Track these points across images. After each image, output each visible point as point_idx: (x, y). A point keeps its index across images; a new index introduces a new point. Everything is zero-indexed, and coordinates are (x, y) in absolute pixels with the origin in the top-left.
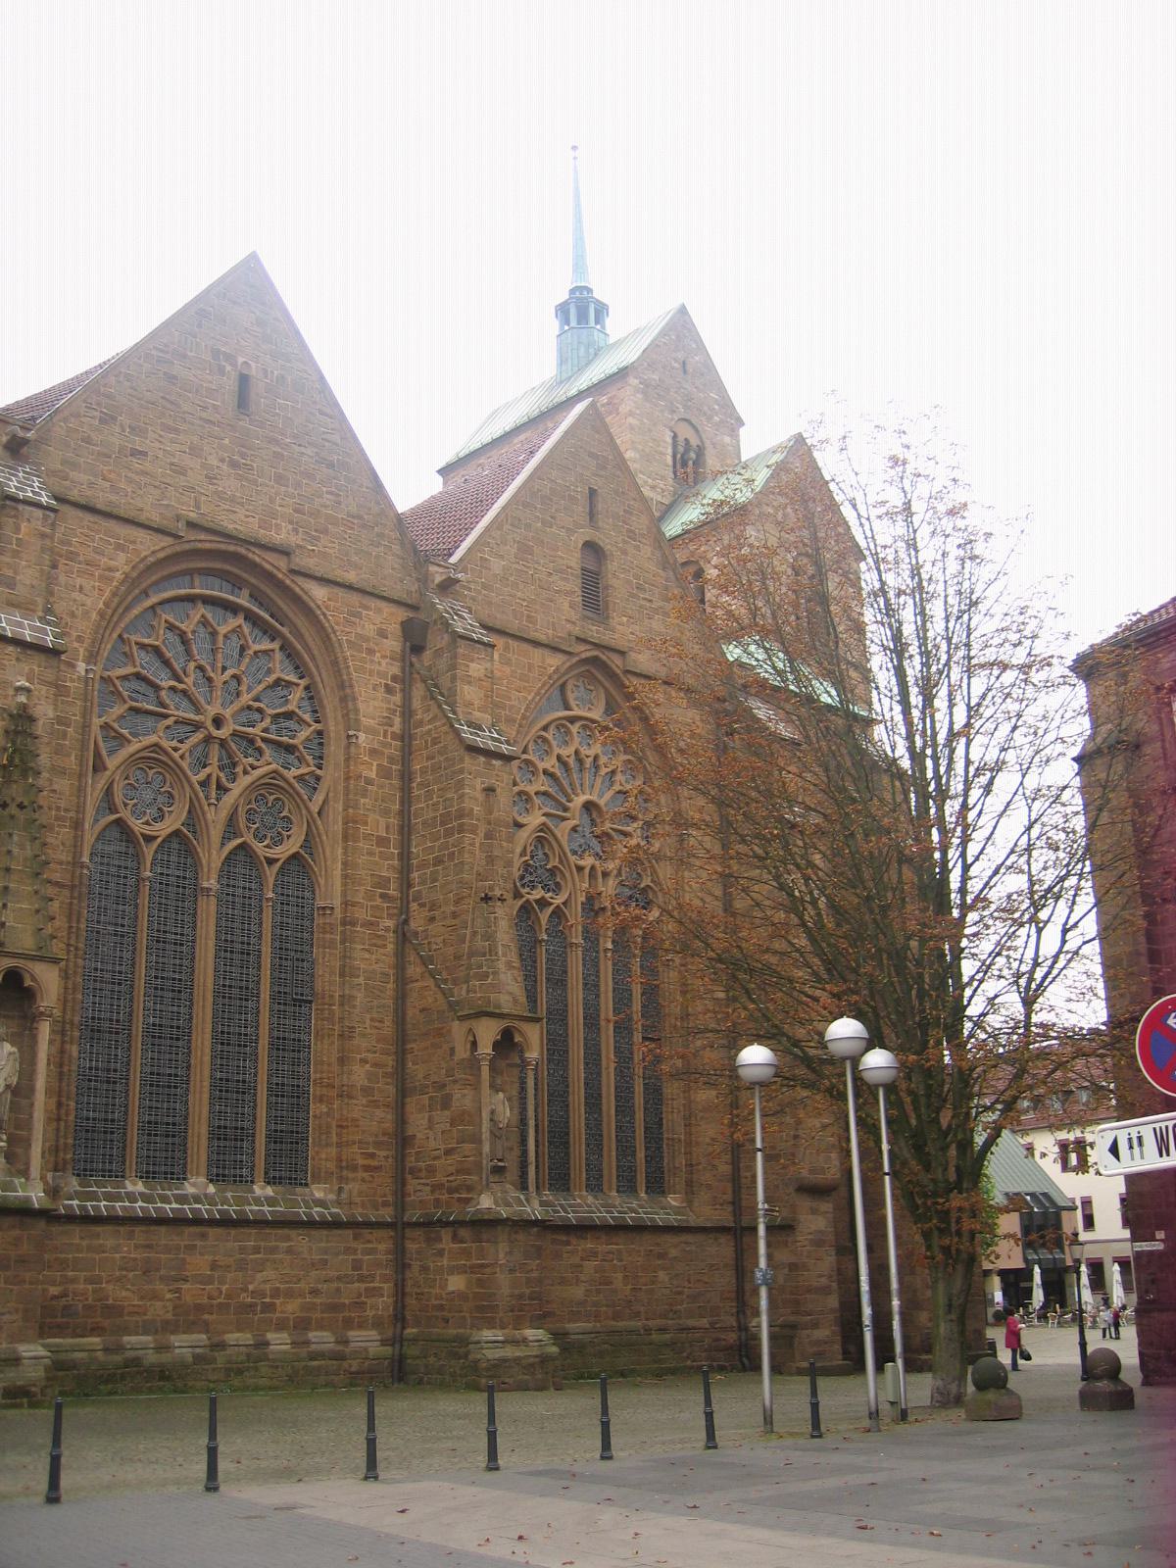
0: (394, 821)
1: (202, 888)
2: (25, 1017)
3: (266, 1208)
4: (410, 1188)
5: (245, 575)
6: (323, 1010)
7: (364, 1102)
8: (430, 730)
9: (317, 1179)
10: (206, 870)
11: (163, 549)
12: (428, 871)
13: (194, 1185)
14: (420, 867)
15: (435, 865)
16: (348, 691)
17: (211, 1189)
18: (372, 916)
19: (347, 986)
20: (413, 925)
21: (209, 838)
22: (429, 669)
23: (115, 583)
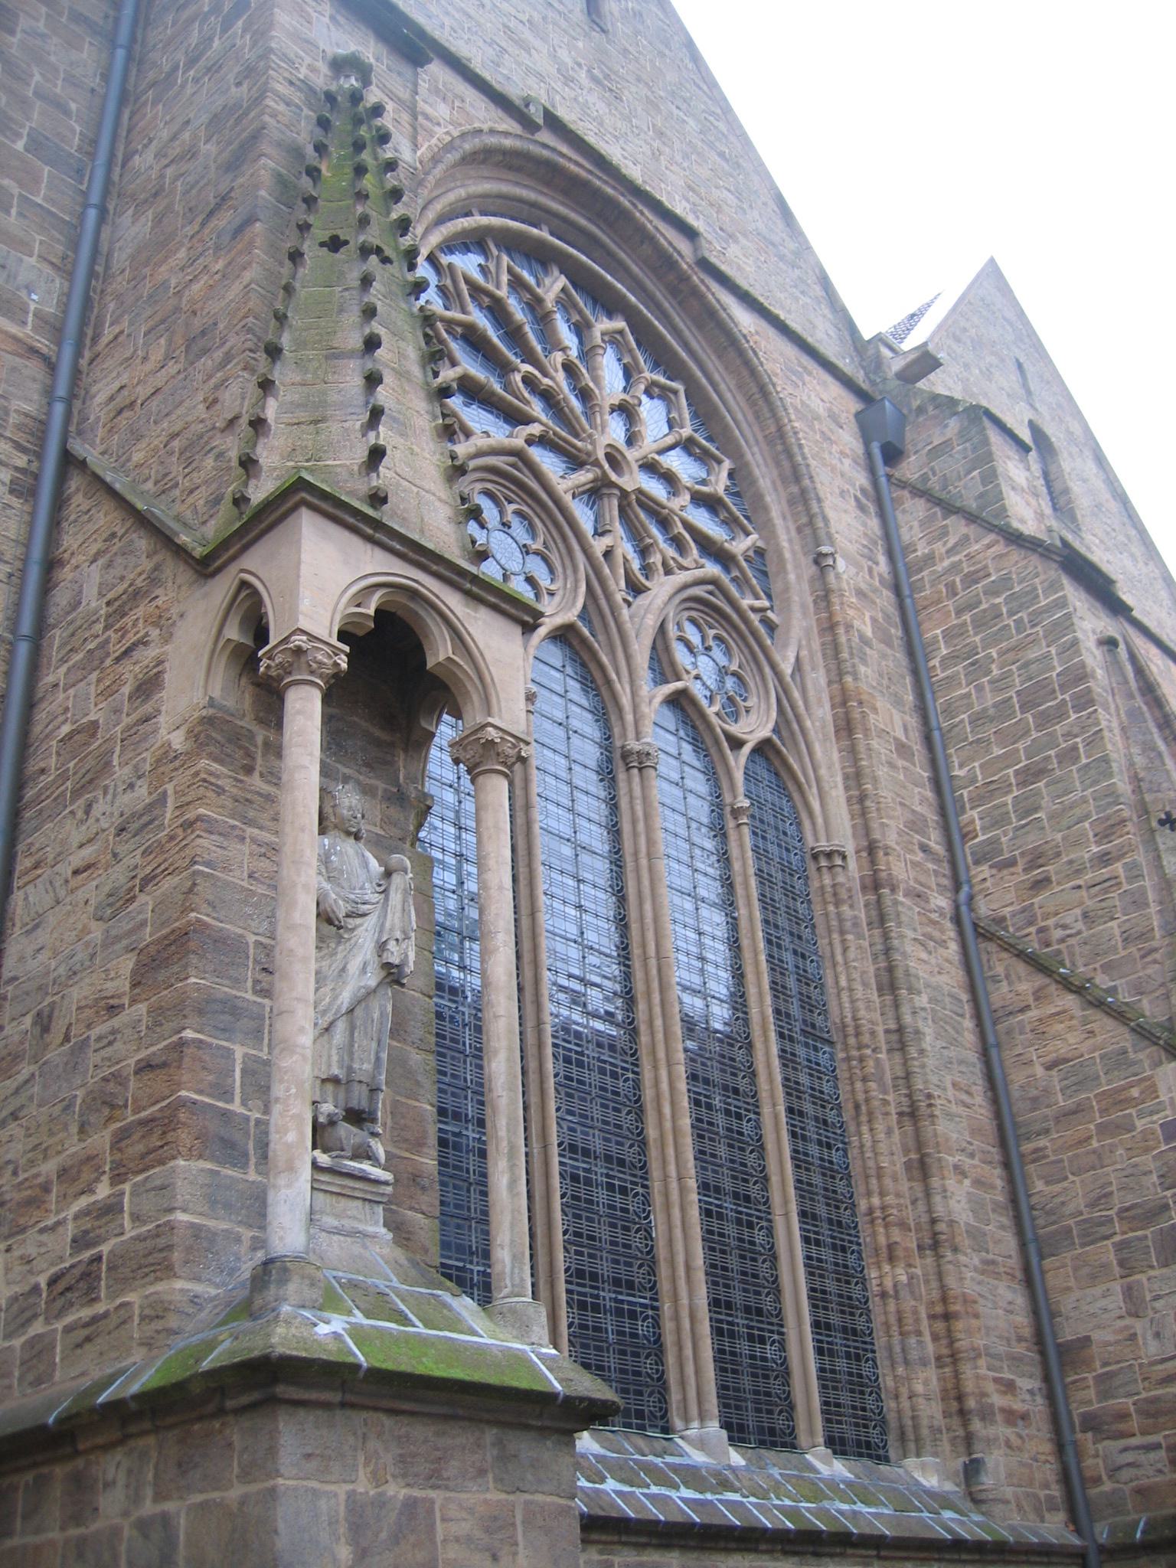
0: (913, 721)
1: (626, 755)
2: (398, 798)
3: (860, 1507)
4: (1093, 1464)
5: (622, 255)
6: (861, 1059)
7: (976, 1261)
8: (955, 567)
9: (912, 1441)
10: (629, 718)
11: (506, 134)
12: (1009, 799)
13: (701, 1444)
14: (977, 801)
15: (1022, 784)
16: (806, 482)
17: (736, 1458)
18: (916, 881)
19: (905, 1010)
20: (983, 908)
21: (628, 658)
22: (925, 478)
23: (434, 141)
